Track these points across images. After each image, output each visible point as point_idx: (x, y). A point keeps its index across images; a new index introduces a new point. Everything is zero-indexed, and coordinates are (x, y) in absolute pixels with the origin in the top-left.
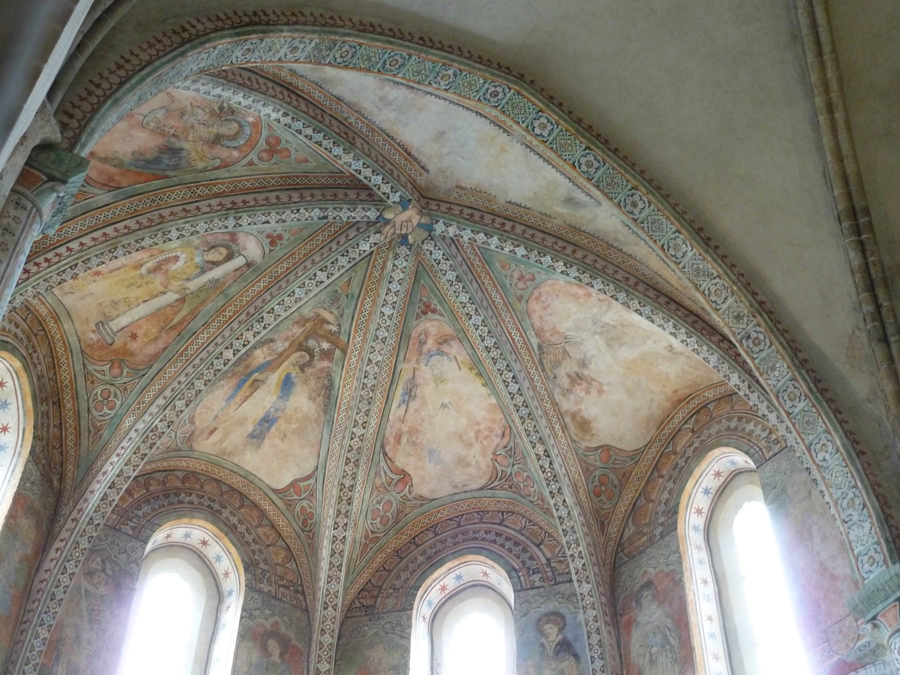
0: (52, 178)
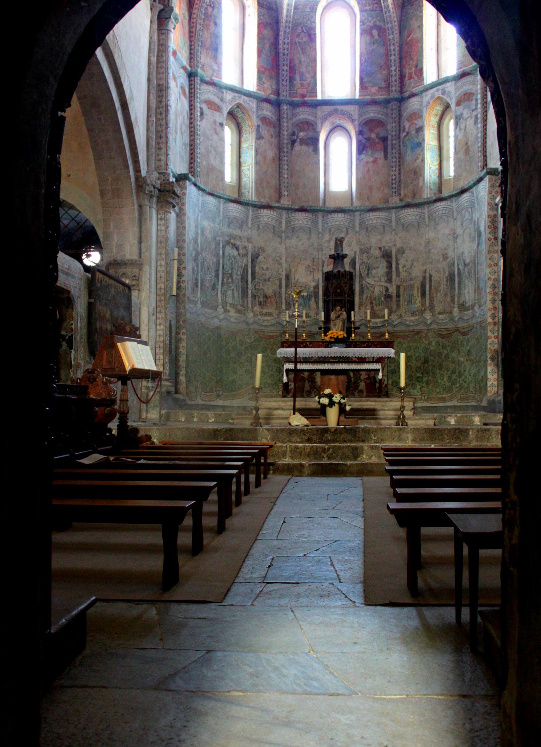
0: (167, 18)
